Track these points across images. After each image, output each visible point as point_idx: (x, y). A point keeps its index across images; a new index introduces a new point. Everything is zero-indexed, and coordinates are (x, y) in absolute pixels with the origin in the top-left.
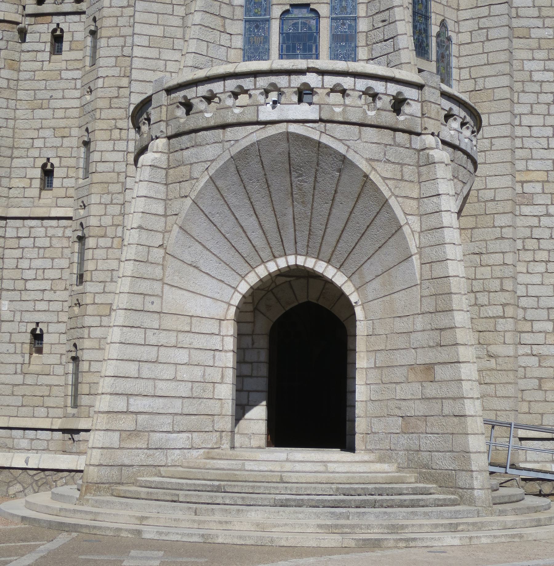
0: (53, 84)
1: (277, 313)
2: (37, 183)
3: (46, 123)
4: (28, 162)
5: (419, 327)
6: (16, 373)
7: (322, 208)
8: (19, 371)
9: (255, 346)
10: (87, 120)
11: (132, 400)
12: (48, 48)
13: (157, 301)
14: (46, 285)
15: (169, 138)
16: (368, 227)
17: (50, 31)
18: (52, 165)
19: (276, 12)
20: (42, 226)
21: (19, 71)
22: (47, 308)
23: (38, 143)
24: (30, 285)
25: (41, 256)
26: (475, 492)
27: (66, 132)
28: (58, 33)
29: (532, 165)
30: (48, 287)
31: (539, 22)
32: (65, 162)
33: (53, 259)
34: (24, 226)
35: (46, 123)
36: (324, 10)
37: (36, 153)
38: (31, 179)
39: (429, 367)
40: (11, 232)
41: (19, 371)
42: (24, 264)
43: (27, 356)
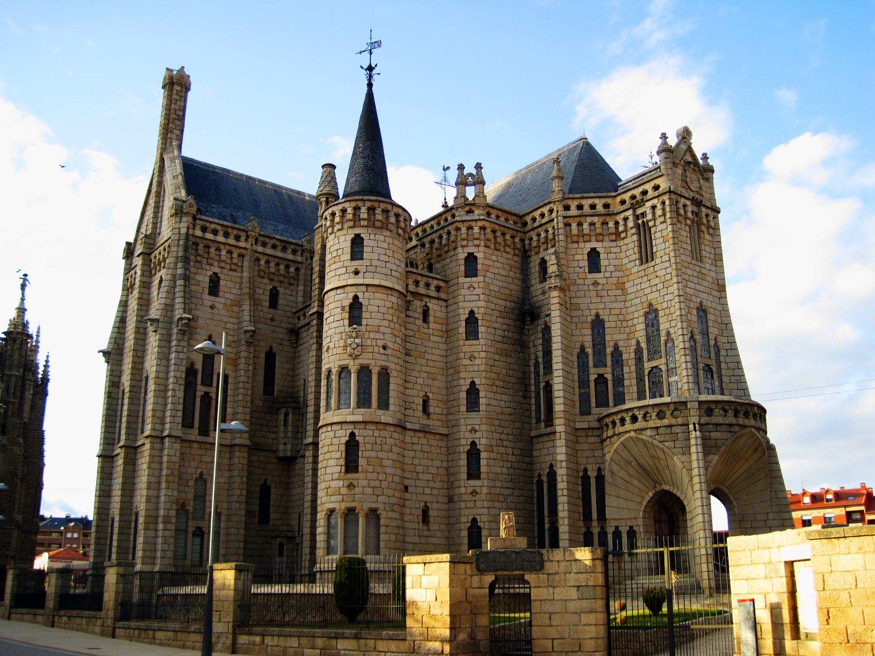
0: (426, 343)
3: (424, 368)
6: (415, 535)
8: (417, 534)
10: (472, 376)
14: (430, 477)
15: (700, 424)
17: (422, 305)
18: (428, 397)
20: (425, 438)
22: (430, 493)
23: (420, 381)
24: (420, 476)
25: (426, 457)
27: (434, 376)
28: (425, 308)
30: (431, 479)
32: (436, 396)
33: (432, 460)
36: (714, 369)
37: (419, 388)
40: (408, 439)
41: (417, 534)
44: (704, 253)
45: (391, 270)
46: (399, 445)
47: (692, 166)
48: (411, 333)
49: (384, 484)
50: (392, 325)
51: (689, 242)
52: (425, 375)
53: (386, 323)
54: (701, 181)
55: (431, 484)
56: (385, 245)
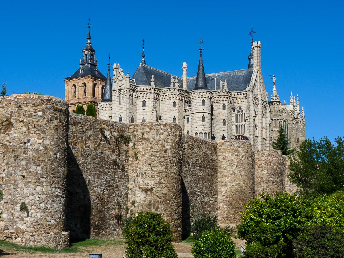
31: (169, 120)
47: (120, 80)
51: (118, 101)
54: (124, 82)
56: (102, 113)
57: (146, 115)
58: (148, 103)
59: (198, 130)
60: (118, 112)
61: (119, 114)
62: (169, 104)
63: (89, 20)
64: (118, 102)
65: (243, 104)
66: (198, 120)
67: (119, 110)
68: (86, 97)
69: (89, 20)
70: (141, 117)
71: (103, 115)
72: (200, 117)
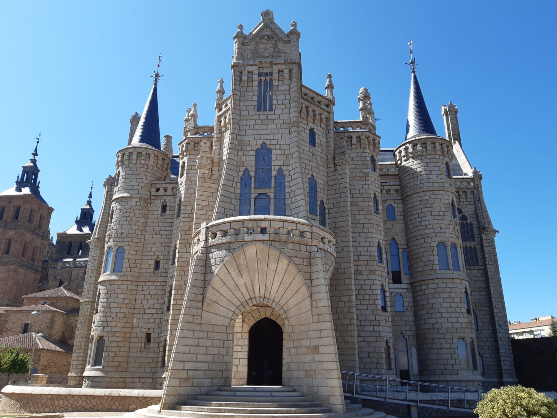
1: (252, 322)
2: (153, 266)
4: (150, 257)
5: (312, 329)
7: (270, 276)
9: (243, 337)
11: (186, 364)
12: (160, 210)
13: (199, 318)
16: (290, 285)
17: (162, 202)
19: (253, 196)
21: (147, 219)
24: (147, 311)
25: (153, 298)
26: (338, 406)
28: (165, 203)
29: (361, 258)
30: (155, 312)
31: (362, 199)
34: (146, 285)
35: (158, 241)
36: (272, 195)
37: (153, 253)
38: (150, 265)
39: (316, 347)
41: (139, 351)
42: (145, 302)
43: (143, 344)
44: (275, 102)
45: (133, 186)
46: (125, 292)
48: (151, 221)
49: (109, 319)
50: (129, 219)
51: (255, 98)
52: (159, 245)
53: (125, 219)
55: (155, 316)
57: (318, 171)
58: (321, 138)
59: (447, 235)
60: (255, 132)
61: (257, 137)
62: (358, 159)
63: (40, 135)
64: (256, 103)
65: (466, 203)
66: (443, 209)
67: (260, 127)
68: (17, 221)
69: (40, 135)
70: (307, 171)
71: (134, 176)
72: (446, 202)
